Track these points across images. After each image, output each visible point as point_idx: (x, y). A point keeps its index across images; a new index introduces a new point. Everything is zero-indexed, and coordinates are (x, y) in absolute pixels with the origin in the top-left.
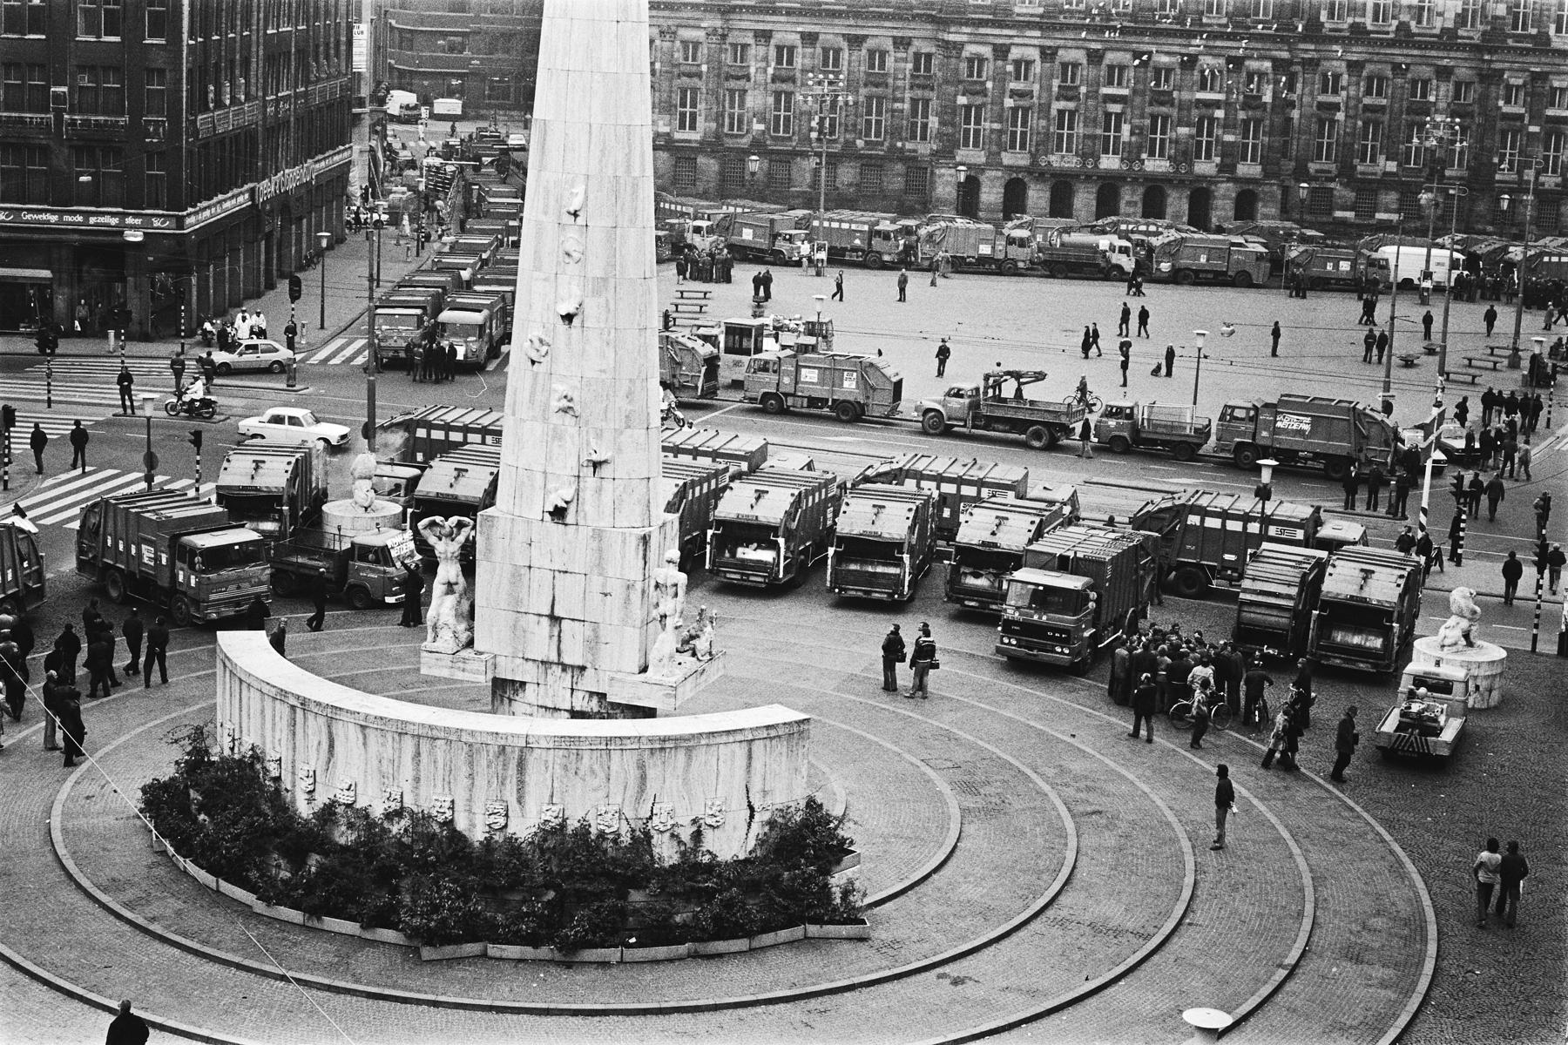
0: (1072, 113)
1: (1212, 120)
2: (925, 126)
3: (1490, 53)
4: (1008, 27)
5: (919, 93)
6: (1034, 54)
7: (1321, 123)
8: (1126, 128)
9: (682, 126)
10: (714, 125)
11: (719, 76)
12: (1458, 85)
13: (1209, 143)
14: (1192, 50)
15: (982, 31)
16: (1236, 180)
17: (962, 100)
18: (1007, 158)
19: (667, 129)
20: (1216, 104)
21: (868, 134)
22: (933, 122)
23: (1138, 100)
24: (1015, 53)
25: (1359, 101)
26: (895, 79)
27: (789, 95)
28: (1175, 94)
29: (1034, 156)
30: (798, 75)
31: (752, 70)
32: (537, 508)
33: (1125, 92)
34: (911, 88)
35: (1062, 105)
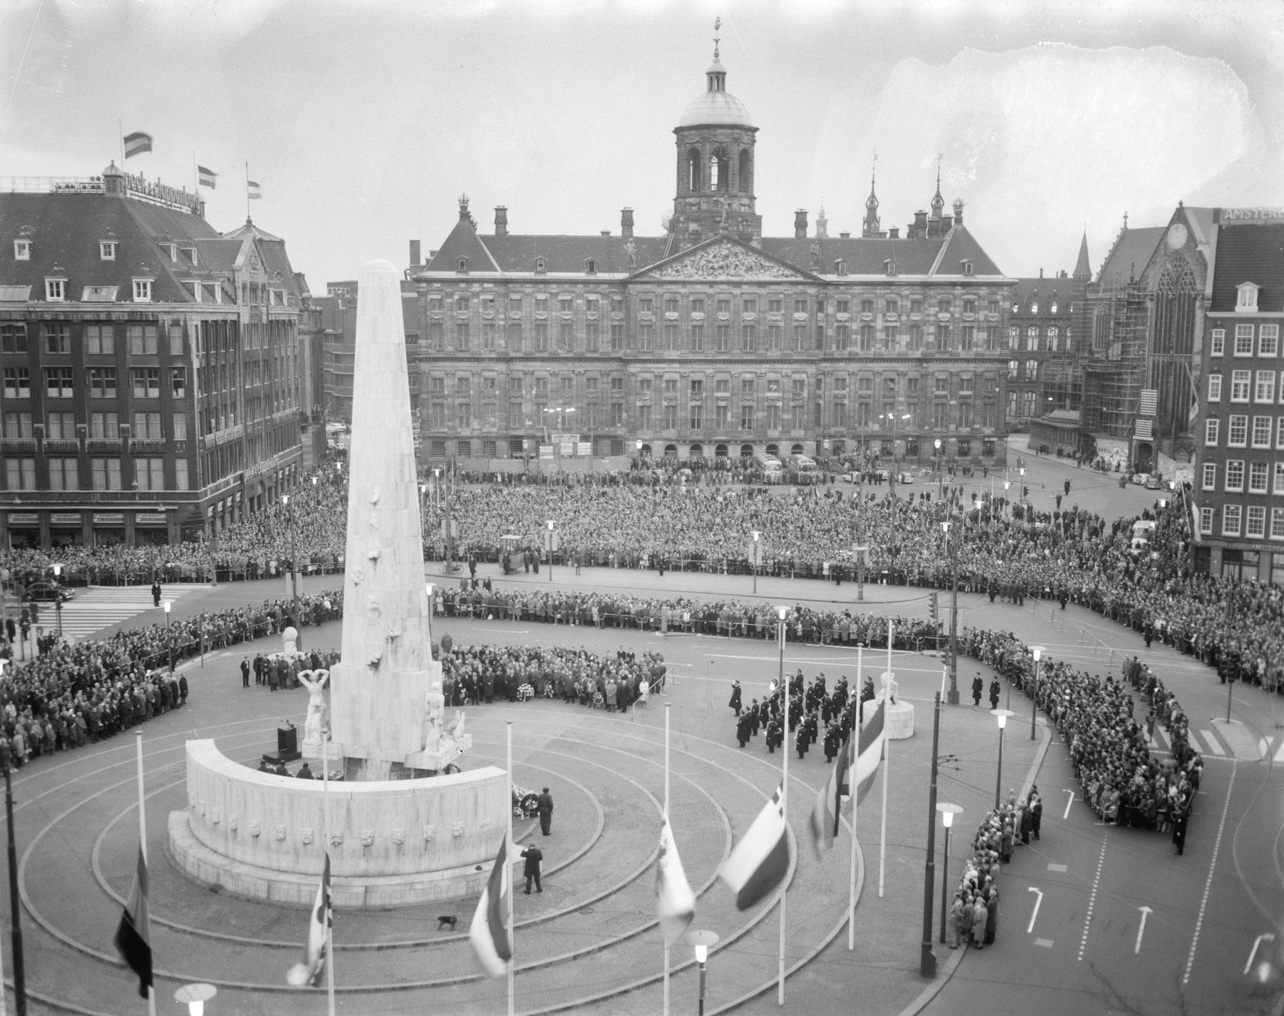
0: (700, 407)
1: (776, 407)
2: (620, 417)
7: (836, 405)
8: (729, 414)
12: (910, 380)
14: (763, 371)
16: (791, 439)
18: (665, 434)
23: (735, 399)
24: (667, 376)
32: (362, 665)
33: (727, 395)
35: (694, 403)
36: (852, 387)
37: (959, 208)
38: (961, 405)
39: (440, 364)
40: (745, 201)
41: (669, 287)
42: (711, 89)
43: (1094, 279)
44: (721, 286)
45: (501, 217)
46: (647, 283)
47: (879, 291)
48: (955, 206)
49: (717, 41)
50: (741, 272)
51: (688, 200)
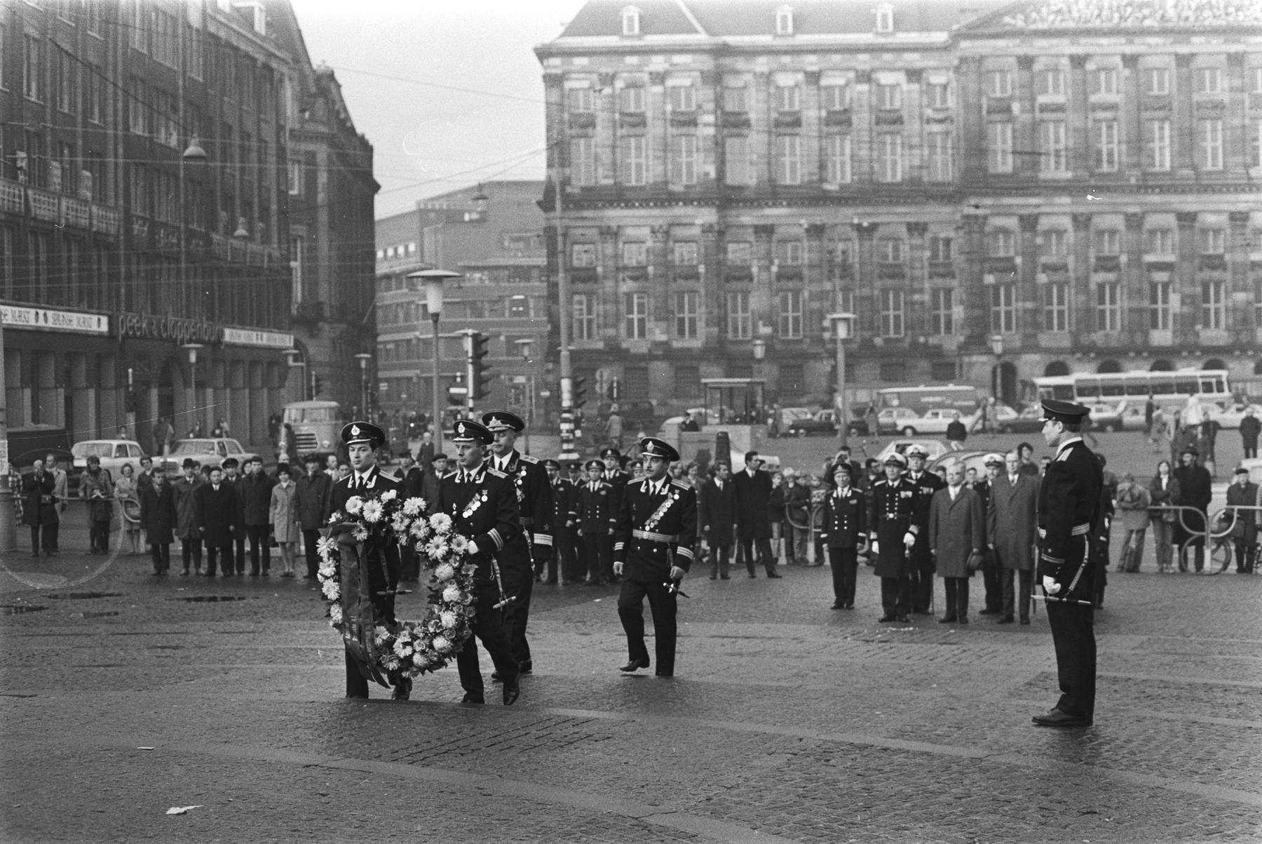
5: (939, 282)
6: (1066, 222)
8: (1175, 301)
9: (681, 332)
10: (715, 330)
11: (718, 275)
15: (1006, 201)
17: (989, 279)
18: (1044, 340)
19: (663, 338)
21: (887, 331)
22: (958, 312)
26: (912, 268)
27: (796, 293)
28: (1227, 257)
29: (1075, 336)
30: (806, 272)
31: (755, 270)
33: (1170, 258)
34: (931, 277)
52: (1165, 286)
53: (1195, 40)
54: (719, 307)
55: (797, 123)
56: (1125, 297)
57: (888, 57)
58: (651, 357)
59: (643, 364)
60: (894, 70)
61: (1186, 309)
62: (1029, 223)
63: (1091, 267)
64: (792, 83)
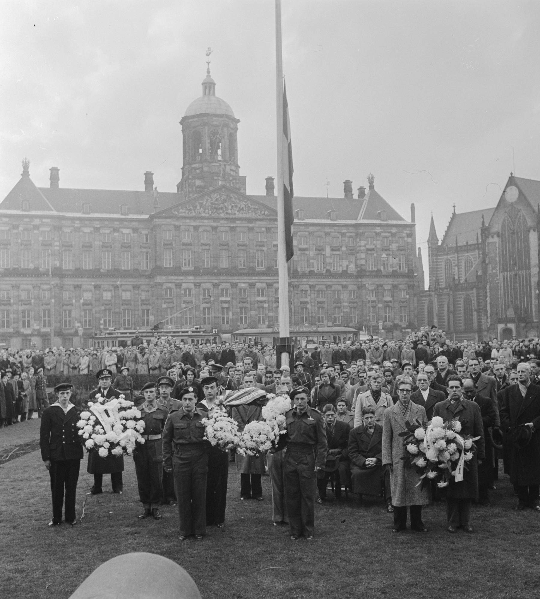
0: (209, 308)
1: (263, 308)
3: (361, 278)
4: (180, 275)
5: (145, 307)
6: (192, 286)
7: (302, 308)
8: (230, 313)
13: (263, 317)
17: (164, 306)
19: (38, 327)
20: (264, 302)
23: (234, 302)
25: (316, 300)
27: (90, 310)
28: (248, 299)
30: (94, 302)
33: (229, 299)
35: (205, 305)
36: (312, 296)
37: (371, 181)
38: (385, 307)
39: (7, 279)
40: (233, 168)
41: (184, 221)
42: (205, 94)
43: (440, 243)
44: (222, 222)
45: (54, 174)
46: (169, 218)
47: (327, 230)
48: (369, 179)
49: (208, 63)
50: (236, 212)
51: (194, 166)
52: (227, 308)
53: (238, 222)
54: (60, 315)
55: (91, 247)
56: (213, 312)
57: (126, 223)
58: (32, 335)
59: (29, 338)
60: (128, 228)
61: (234, 317)
62: (179, 285)
63: (201, 302)
64: (89, 231)
